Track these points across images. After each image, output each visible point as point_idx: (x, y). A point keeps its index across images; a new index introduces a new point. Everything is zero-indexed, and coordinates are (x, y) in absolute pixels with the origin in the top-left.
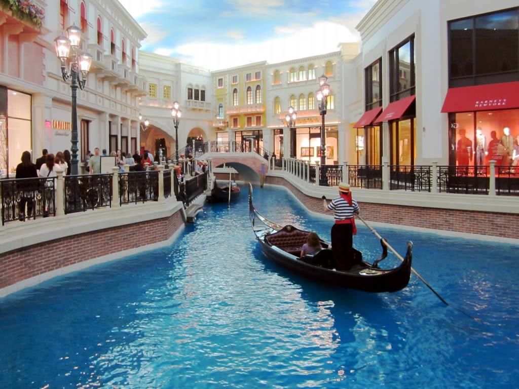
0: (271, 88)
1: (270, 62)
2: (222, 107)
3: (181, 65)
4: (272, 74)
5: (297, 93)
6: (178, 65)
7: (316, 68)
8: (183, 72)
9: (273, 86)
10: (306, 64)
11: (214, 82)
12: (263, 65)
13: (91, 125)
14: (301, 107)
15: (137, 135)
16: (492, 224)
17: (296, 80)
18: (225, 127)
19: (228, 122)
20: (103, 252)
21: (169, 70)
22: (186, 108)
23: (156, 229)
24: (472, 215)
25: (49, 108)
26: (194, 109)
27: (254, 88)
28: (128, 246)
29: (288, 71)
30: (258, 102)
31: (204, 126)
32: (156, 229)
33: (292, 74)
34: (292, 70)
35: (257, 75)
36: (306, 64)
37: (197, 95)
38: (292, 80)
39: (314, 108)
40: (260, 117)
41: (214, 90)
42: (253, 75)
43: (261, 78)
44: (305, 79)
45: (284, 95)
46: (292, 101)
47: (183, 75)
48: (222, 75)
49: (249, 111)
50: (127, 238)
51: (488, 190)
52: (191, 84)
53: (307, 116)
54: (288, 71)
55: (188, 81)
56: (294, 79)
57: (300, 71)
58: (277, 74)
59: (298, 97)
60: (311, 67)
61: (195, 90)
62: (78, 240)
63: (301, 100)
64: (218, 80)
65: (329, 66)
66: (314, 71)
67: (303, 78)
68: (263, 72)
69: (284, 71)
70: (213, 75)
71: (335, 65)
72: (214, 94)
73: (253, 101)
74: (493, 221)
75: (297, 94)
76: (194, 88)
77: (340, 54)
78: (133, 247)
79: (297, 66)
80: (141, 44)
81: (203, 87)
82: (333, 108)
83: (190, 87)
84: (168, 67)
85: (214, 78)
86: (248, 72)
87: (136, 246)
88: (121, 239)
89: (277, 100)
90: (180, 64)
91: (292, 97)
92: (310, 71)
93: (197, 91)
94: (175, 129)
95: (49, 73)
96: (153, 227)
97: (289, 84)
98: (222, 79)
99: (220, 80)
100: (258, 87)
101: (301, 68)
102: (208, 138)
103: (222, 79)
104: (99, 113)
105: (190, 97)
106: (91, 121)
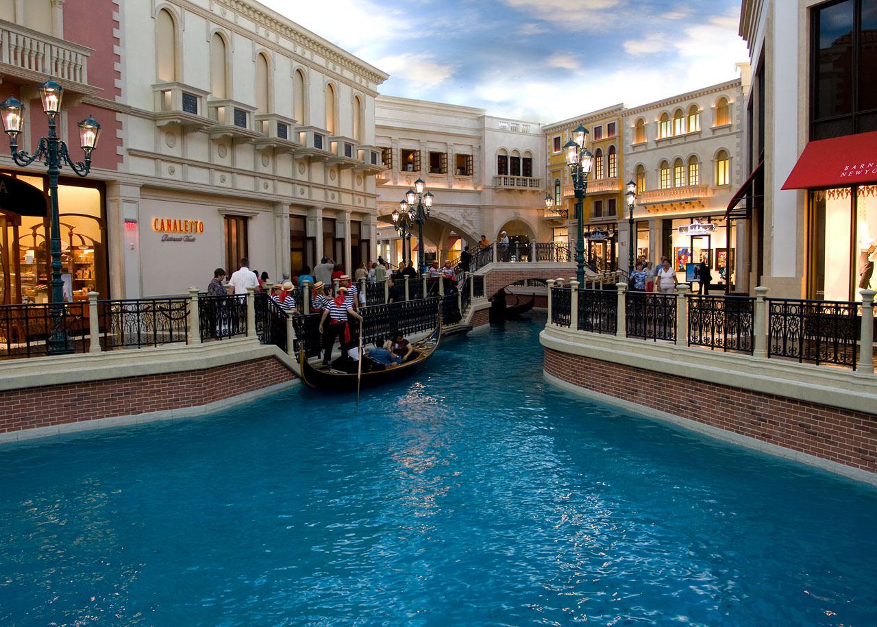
0: (631, 151)
1: (630, 104)
2: (559, 185)
3: (486, 118)
4: (633, 126)
5: (670, 155)
6: (481, 119)
7: (701, 112)
8: (490, 129)
9: (634, 147)
10: (684, 105)
11: (548, 144)
12: (617, 110)
13: (253, 226)
14: (678, 181)
15: (345, 234)
16: (753, 413)
17: (669, 135)
18: (562, 218)
19: (567, 211)
20: (64, 418)
21: (465, 128)
22: (495, 189)
23: (178, 388)
24: (726, 393)
25: (135, 202)
26: (509, 190)
27: (605, 152)
28: (115, 413)
29: (657, 120)
30: (612, 175)
31: (530, 216)
32: (178, 388)
33: (664, 124)
34: (664, 117)
35: (611, 128)
36: (684, 105)
37: (515, 167)
38: (664, 136)
39: (668, 187)
40: (615, 200)
41: (548, 157)
42: (605, 130)
43: (616, 134)
44: (684, 132)
45: (650, 161)
46: (664, 172)
47: (488, 137)
48: (559, 132)
49: (596, 191)
50: (113, 399)
51: (858, 343)
52: (504, 150)
53: (683, 198)
54: (657, 120)
55: (493, 148)
56: (665, 133)
57: (676, 117)
58: (640, 127)
59: (671, 165)
60: (693, 110)
61: (524, 159)
62: (10, 399)
63: (678, 170)
64: (553, 141)
65: (722, 108)
66: (698, 116)
67: (680, 130)
68: (619, 122)
69: (652, 118)
70: (546, 132)
71: (732, 104)
72: (548, 164)
73: (605, 176)
74: (755, 409)
75: (671, 160)
76: (510, 154)
77: (740, 83)
78: (127, 412)
79: (670, 109)
80: (378, 91)
81: (528, 152)
82: (727, 182)
83: (503, 154)
84: (463, 125)
85: (548, 137)
86: (597, 124)
87: (134, 411)
88: (102, 401)
89: (640, 170)
90: (484, 117)
91: (664, 164)
92: (692, 118)
93: (515, 160)
94: (69, 237)
95: (129, 150)
96: (169, 385)
97: (657, 142)
98: (559, 138)
99: (557, 140)
100: (612, 150)
101: (679, 113)
102: (539, 236)
103: (559, 138)
104: (273, 204)
105: (502, 168)
106: (251, 218)
